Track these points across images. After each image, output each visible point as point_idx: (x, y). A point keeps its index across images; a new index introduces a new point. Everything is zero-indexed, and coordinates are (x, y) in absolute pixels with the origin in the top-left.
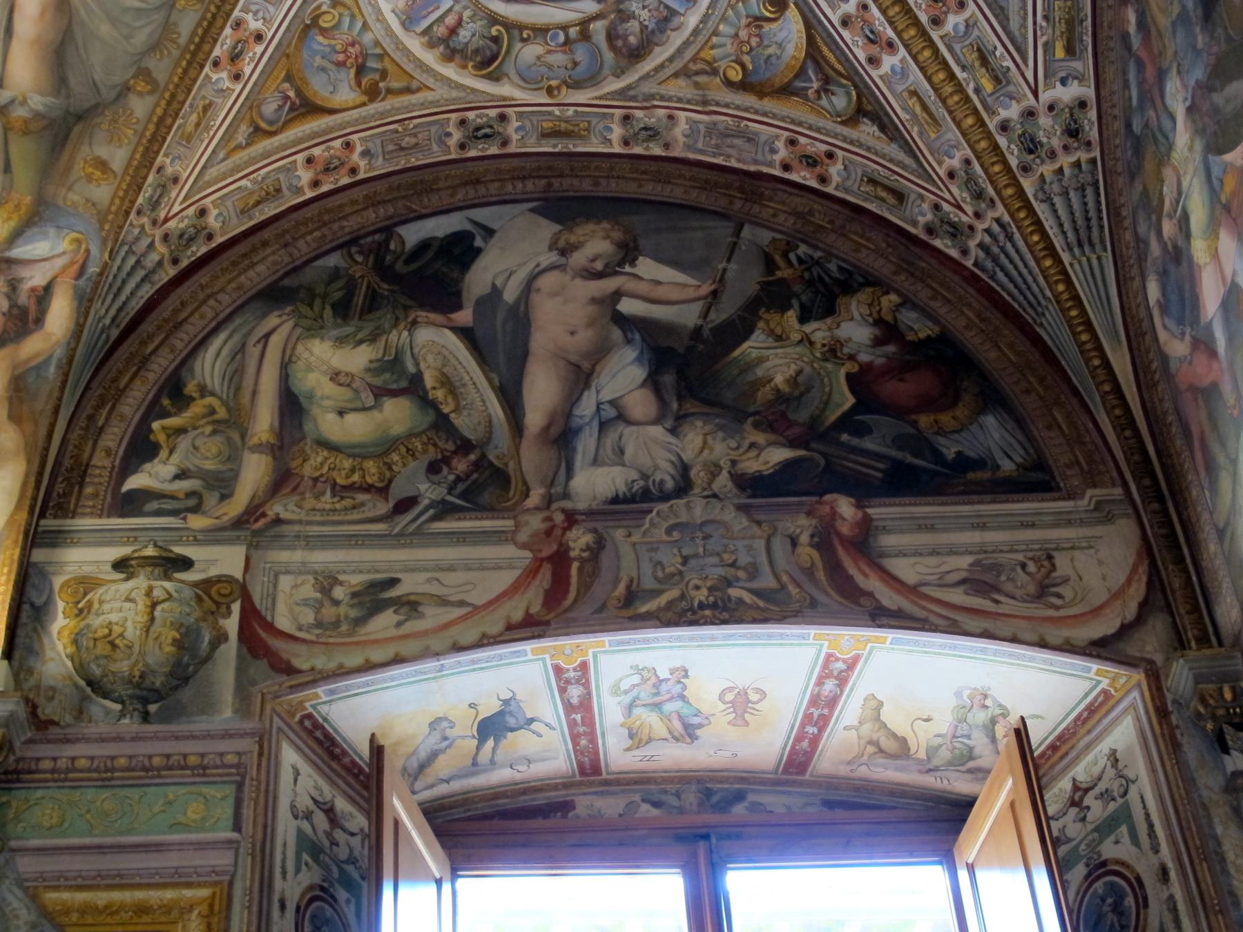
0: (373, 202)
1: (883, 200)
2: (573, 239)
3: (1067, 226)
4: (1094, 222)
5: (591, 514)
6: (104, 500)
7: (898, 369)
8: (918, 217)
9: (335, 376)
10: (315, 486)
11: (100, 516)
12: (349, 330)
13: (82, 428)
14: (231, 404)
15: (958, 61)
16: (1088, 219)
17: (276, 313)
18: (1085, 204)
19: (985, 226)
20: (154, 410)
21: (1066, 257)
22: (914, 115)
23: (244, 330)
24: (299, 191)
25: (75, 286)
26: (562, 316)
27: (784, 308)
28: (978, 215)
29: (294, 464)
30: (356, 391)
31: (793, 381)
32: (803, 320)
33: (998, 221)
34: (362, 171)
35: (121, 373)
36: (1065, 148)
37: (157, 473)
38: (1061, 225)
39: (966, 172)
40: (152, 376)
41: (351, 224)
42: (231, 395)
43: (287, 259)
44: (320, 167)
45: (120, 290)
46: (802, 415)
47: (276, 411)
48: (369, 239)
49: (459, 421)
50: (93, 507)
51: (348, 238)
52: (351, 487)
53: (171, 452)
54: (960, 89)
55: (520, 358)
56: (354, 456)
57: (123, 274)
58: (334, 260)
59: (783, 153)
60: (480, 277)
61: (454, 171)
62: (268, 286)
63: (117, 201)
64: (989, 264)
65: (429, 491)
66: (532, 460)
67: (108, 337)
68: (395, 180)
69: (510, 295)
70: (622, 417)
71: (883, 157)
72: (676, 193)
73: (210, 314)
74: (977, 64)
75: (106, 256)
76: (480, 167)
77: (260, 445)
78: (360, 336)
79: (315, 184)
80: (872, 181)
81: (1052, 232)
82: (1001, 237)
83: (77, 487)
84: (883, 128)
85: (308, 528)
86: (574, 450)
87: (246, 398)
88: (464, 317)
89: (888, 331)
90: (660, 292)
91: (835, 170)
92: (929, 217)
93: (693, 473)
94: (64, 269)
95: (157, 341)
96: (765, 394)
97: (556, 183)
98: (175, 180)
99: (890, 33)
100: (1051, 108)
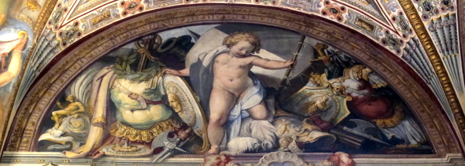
0: (149, 22)
1: (364, 28)
2: (233, 40)
3: (442, 42)
4: (454, 41)
5: (236, 157)
6: (31, 144)
7: (368, 100)
8: (379, 36)
9: (130, 95)
10: (120, 141)
11: (29, 151)
12: (137, 75)
13: (22, 113)
14: (86, 105)
16: (451, 40)
17: (106, 68)
18: (450, 33)
19: (408, 41)
20: (53, 107)
21: (441, 55)
23: (93, 74)
24: (118, 16)
25: (22, 53)
26: (227, 73)
27: (321, 73)
28: (404, 36)
29: (112, 132)
30: (139, 101)
31: (324, 104)
32: (329, 78)
34: (145, 9)
35: (40, 90)
37: (54, 134)
38: (440, 42)
39: (400, 18)
40: (53, 93)
41: (140, 31)
42: (86, 102)
43: (112, 45)
44: (127, 6)
45: (40, 55)
46: (327, 118)
47: (105, 109)
48: (147, 38)
49: (182, 116)
50: (26, 147)
51: (138, 37)
52: (135, 142)
53: (60, 125)
55: (209, 90)
56: (137, 129)
57: (42, 49)
58: (131, 46)
59: (323, 7)
60: (193, 56)
61: (184, 10)
62: (103, 56)
63: (41, 18)
64: (408, 57)
65: (168, 145)
66: (212, 133)
67: (35, 75)
68: (158, 13)
69: (205, 63)
70: (251, 116)
71: (365, 10)
72: (277, 22)
73: (78, 67)
75: (35, 41)
76: (195, 8)
77: (98, 123)
78: (141, 78)
79: (125, 13)
80: (360, 20)
81: (436, 44)
82: (414, 46)
83: (20, 138)
85: (117, 159)
86: (230, 129)
87: (92, 103)
88: (186, 72)
89: (365, 84)
90: (269, 64)
91: (345, 15)
92: (384, 36)
93: (280, 141)
94: (18, 46)
95: (55, 78)
96: (312, 109)
97: (227, 17)
98: (66, 10)
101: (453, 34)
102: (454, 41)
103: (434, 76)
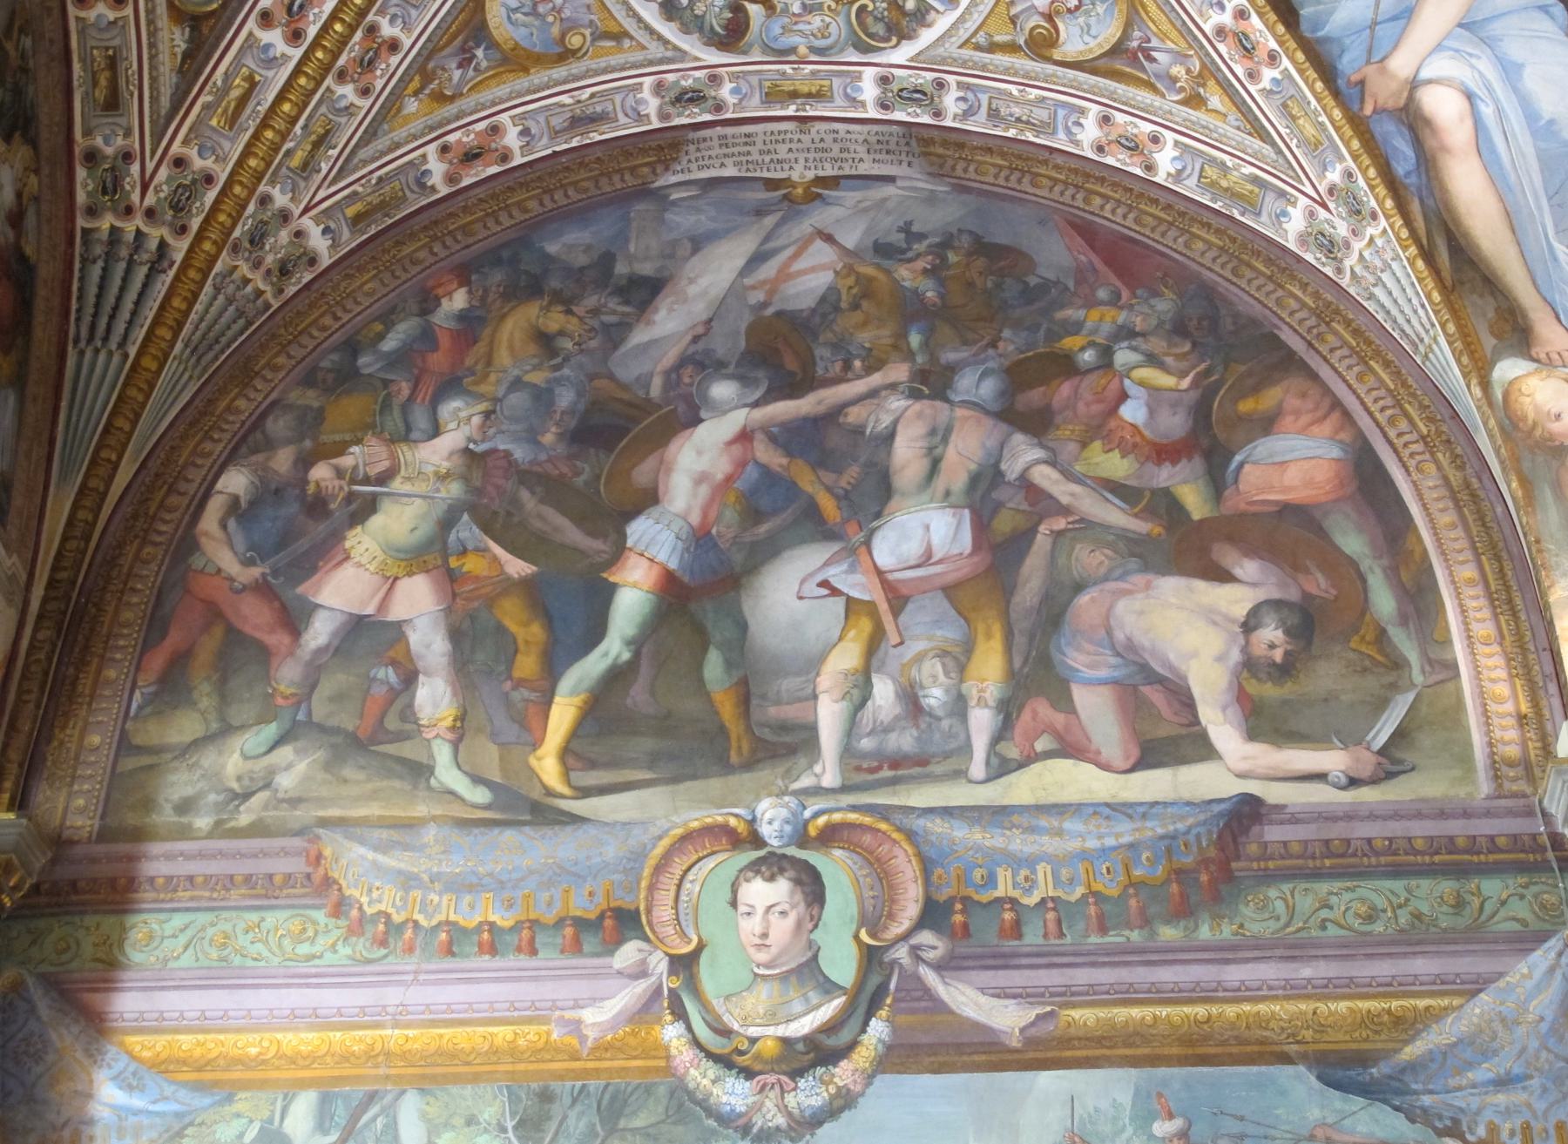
1: (95, 84)
4: (217, 347)
15: (310, 117)
18: (229, 328)
19: (145, 229)
21: (179, 346)
22: (227, 88)
28: (150, 213)
33: (163, 245)
36: (269, 272)
38: (201, 320)
39: (194, 182)
54: (284, 136)
64: (98, 250)
71: (152, 67)
74: (313, 137)
80: (113, 63)
81: (193, 316)
84: (187, 55)
92: (109, 151)
99: (312, 31)
100: (299, 234)
101: (230, 333)
102: (217, 347)
103: (116, 359)
